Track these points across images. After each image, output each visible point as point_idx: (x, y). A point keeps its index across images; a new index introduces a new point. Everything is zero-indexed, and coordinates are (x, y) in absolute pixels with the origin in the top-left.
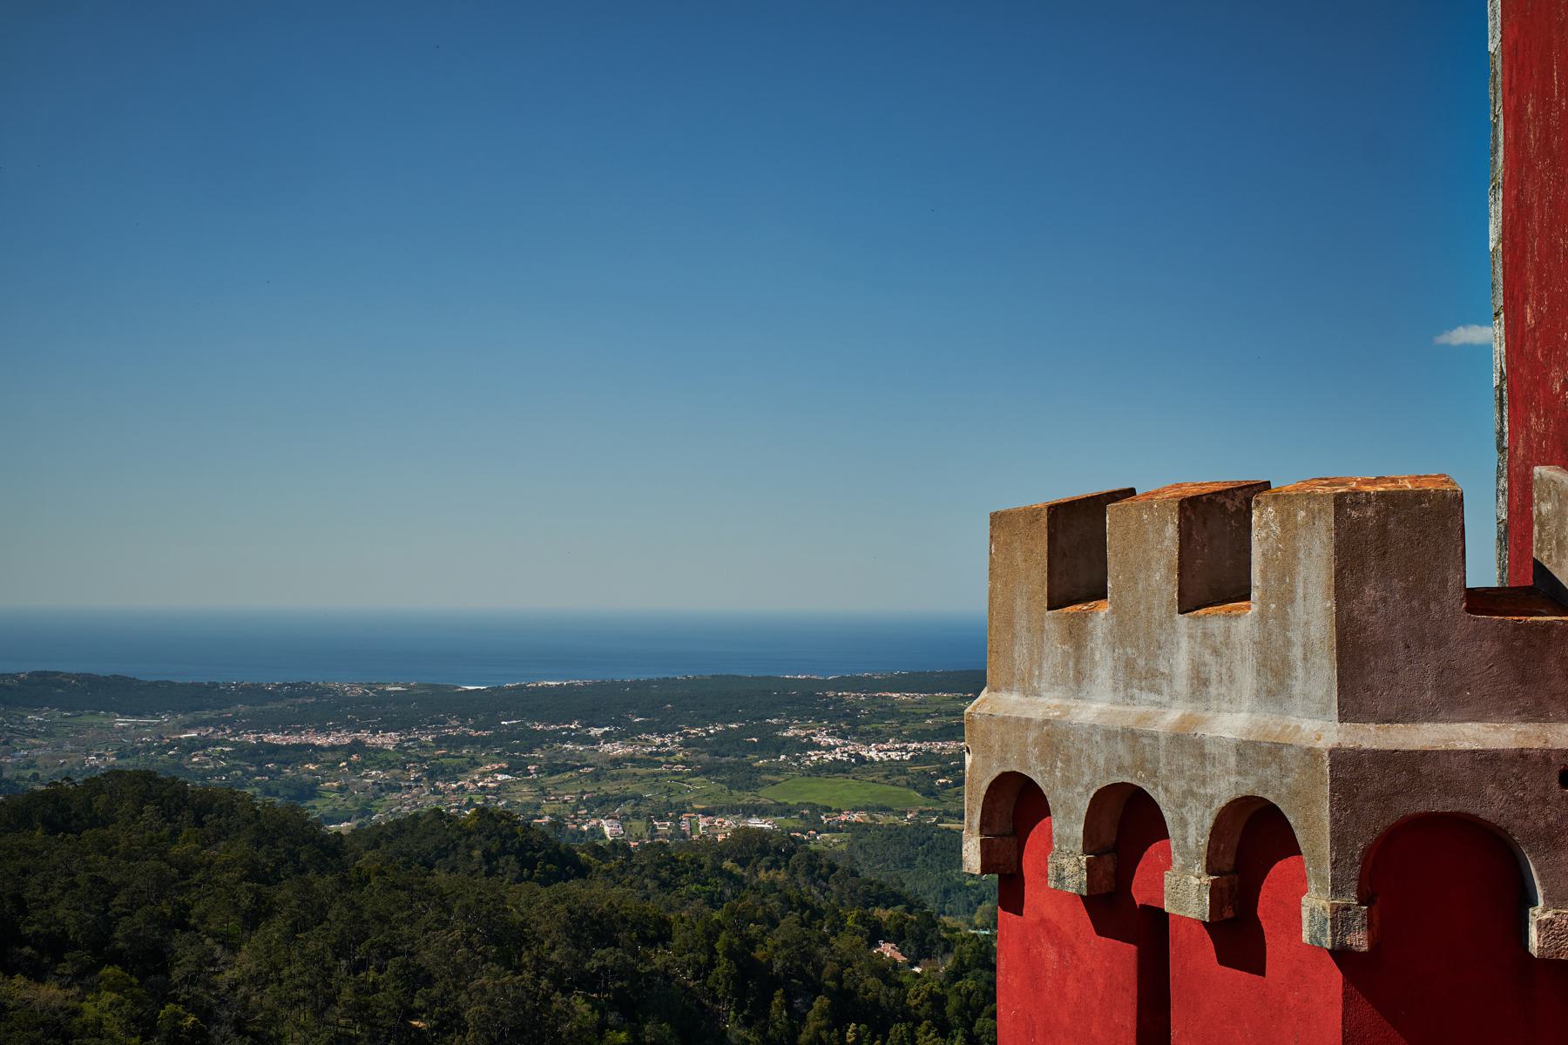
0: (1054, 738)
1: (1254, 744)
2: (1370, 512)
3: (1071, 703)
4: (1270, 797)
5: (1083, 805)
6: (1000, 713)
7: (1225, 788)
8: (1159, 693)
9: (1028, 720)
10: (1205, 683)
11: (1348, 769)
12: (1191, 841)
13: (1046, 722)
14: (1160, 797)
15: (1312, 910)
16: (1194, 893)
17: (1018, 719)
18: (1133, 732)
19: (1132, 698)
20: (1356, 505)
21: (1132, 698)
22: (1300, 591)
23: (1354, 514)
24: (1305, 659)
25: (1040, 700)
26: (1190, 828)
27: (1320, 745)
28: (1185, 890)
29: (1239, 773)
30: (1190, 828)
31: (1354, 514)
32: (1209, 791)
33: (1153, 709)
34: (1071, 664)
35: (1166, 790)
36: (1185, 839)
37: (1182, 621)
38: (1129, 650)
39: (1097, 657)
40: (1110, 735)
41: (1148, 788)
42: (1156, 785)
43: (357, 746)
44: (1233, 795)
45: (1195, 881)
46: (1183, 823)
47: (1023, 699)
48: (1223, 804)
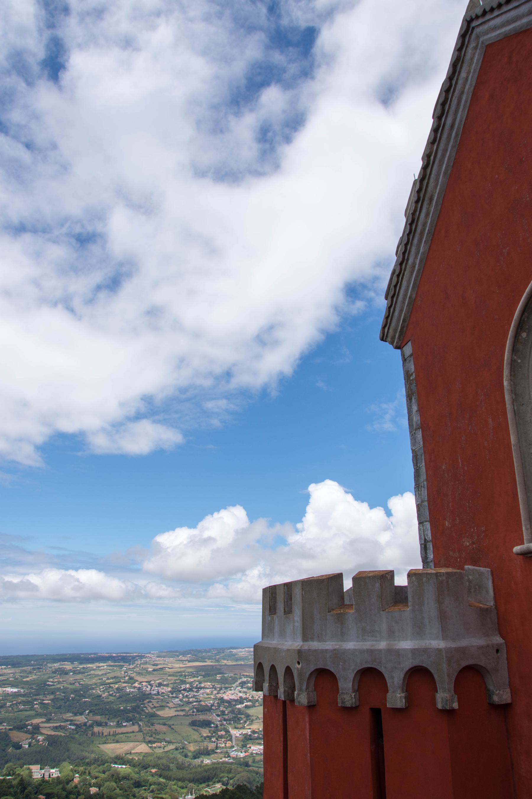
0: (337, 655)
1: (417, 649)
2: (444, 578)
3: (342, 643)
4: (424, 665)
5: (351, 676)
6: (314, 648)
7: (407, 665)
8: (376, 637)
9: (326, 650)
10: (393, 632)
11: (452, 654)
12: (396, 683)
13: (335, 650)
14: (383, 670)
15: (442, 698)
16: (399, 700)
17: (322, 650)
18: (371, 650)
19: (365, 639)
20: (441, 576)
21: (365, 639)
22: (426, 602)
23: (441, 579)
24: (430, 622)
25: (327, 643)
26: (395, 679)
27: (440, 647)
28: (396, 698)
29: (413, 659)
30: (395, 679)
31: (441, 579)
32: (402, 666)
33: (374, 642)
34: (339, 630)
35: (385, 667)
36: (393, 682)
37: (383, 614)
38: (363, 624)
39: (350, 627)
40: (362, 652)
41: (378, 668)
42: (381, 666)
43: (218, 661)
44: (411, 666)
45: (399, 695)
46: (392, 677)
47: (319, 643)
48: (407, 669)
